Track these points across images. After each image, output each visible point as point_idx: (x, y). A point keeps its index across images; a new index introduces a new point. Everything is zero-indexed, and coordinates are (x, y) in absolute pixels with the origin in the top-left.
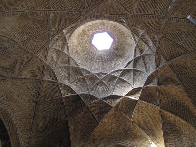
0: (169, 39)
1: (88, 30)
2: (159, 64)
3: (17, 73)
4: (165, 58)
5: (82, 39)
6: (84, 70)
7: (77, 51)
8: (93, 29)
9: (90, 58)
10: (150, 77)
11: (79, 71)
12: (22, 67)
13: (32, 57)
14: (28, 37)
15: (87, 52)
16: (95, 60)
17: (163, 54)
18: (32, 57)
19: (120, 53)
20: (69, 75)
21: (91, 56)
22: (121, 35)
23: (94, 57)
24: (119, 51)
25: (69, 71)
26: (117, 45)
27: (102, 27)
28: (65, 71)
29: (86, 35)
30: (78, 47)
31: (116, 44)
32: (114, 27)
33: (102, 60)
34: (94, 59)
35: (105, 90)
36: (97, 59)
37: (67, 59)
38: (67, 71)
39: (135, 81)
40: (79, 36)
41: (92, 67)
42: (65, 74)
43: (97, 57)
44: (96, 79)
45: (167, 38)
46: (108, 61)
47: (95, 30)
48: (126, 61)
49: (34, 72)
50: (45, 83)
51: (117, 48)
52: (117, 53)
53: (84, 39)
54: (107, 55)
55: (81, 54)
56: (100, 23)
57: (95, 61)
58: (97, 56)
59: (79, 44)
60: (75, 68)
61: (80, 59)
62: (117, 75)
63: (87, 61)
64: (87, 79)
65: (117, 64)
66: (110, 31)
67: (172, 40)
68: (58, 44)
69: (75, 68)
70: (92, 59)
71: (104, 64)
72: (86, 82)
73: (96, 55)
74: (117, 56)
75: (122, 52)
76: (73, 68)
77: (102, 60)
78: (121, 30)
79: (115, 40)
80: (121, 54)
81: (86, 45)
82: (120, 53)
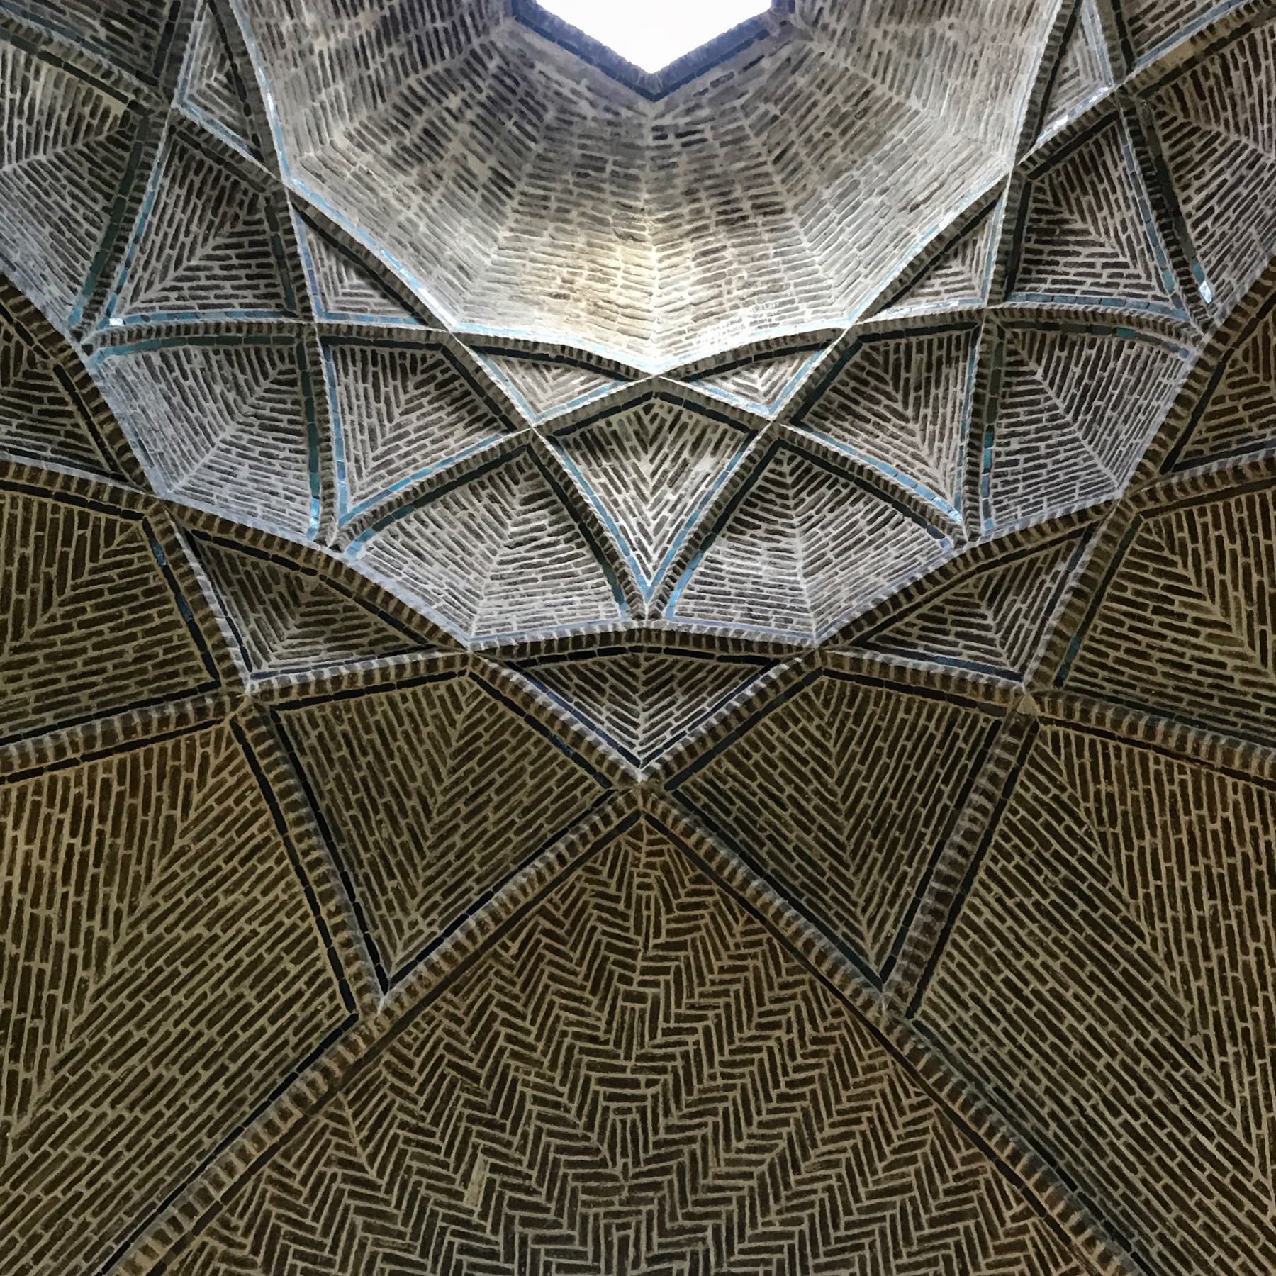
0: (1007, 792)
2: (592, 686)
4: (697, 757)
10: (310, 582)
17: (741, 732)
19: (461, 134)
22: (722, 191)
24: (488, 126)
26: (567, 117)
31: (584, 107)
32: (839, 120)
39: (156, 359)
45: (1021, 776)
48: (379, 217)
51: (531, 107)
52: (454, 102)
67: (1001, 826)
74: (415, 102)
75: (482, 172)
78: (790, 204)
79: (643, 104)
80: (454, 147)
82: (461, 134)
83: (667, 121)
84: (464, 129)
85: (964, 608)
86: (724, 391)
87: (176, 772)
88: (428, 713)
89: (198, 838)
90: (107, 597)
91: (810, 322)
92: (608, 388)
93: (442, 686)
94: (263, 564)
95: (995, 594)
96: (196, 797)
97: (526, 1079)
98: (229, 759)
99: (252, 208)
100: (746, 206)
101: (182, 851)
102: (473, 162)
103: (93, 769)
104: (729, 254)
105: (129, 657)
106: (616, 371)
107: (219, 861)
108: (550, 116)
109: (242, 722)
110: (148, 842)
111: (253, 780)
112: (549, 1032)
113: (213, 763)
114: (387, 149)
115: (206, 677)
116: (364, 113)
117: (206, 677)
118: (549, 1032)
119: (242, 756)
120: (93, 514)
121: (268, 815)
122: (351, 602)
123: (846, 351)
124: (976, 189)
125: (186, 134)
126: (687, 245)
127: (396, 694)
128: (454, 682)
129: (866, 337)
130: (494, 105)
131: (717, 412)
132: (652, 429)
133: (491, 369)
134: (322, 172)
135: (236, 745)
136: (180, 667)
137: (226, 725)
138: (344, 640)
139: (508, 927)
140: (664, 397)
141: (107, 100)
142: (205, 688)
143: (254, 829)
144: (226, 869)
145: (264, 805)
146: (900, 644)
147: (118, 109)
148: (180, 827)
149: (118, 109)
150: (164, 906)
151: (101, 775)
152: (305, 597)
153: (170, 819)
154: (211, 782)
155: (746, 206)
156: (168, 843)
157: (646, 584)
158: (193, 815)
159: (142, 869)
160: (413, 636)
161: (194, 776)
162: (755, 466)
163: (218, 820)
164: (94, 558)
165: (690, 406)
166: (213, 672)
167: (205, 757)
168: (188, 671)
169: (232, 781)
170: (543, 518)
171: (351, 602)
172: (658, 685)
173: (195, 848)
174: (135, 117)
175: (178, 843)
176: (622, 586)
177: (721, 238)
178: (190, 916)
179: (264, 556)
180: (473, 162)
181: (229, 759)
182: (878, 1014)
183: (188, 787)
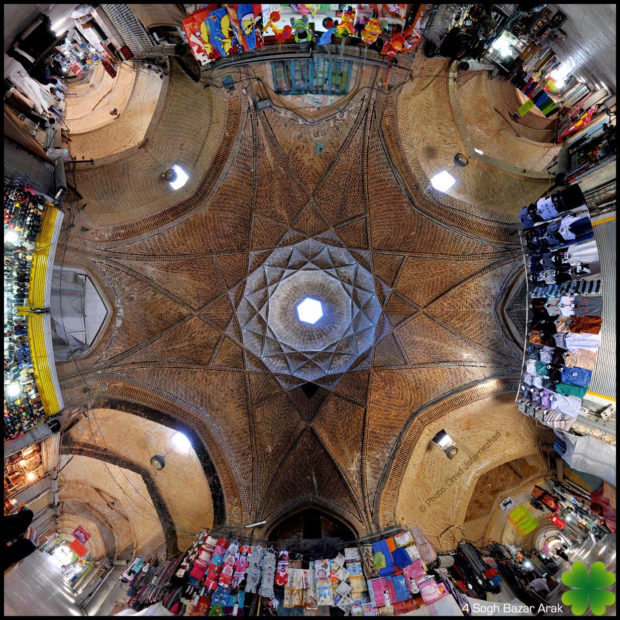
3: (206, 360)
4: (363, 249)
5: (286, 320)
6: (307, 353)
12: (211, 351)
14: (205, 302)
15: (301, 333)
16: (316, 337)
19: (337, 311)
20: (288, 365)
22: (323, 289)
23: (312, 334)
24: (334, 310)
25: (286, 359)
30: (286, 331)
36: (317, 335)
40: (281, 318)
43: (316, 333)
44: (329, 356)
46: (331, 330)
47: (294, 301)
50: (252, 377)
53: (289, 319)
55: (294, 337)
61: (295, 344)
62: (351, 332)
64: (317, 361)
65: (343, 325)
72: (316, 365)
73: (313, 331)
74: (337, 317)
76: (290, 355)
82: (337, 311)
85: (331, 241)
86: (335, 275)
91: (325, 274)
92: (345, 284)
95: (328, 239)
97: (402, 237)
106: (343, 284)
112: (397, 239)
118: (397, 239)
124: (303, 272)
125: (354, 331)
129: (321, 268)
133: (351, 294)
134: (348, 319)
138: (381, 286)
139: (391, 250)
146: (339, 242)
157: (353, 267)
172: (362, 257)
176: (357, 268)
182: (368, 215)
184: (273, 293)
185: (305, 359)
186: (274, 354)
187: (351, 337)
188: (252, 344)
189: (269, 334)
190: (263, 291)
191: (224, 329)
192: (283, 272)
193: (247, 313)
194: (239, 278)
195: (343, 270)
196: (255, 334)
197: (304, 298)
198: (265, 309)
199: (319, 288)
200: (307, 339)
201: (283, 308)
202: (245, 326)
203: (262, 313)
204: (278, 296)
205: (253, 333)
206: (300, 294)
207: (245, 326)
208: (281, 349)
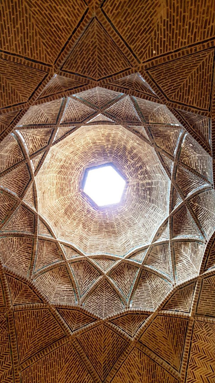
1: (96, 222)
7: (144, 226)
8: (88, 216)
9: (148, 192)
11: (178, 213)
13: (138, 349)
18: (138, 349)
21: (145, 191)
27: (77, 206)
28: (182, 251)
29: (108, 221)
30: (136, 227)
32: (62, 189)
33: (141, 167)
34: (148, 184)
35: (191, 145)
36: (145, 178)
37: (158, 247)
38: (183, 246)
41: (161, 184)
42: (189, 251)
43: (141, 180)
46: (136, 155)
47: (88, 211)
49: (176, 337)
53: (117, 219)
54: (127, 161)
55: (147, 215)
56: (71, 213)
57: (150, 181)
58: (138, 180)
59: (130, 226)
60: (174, 225)
63: (157, 198)
64: (188, 191)
66: (75, 188)
68: (128, 280)
69: (174, 225)
70: (150, 189)
71: (145, 159)
77: (141, 167)
78: (58, 176)
79: (87, 167)
80: (104, 141)
81: (127, 210)
83: (82, 168)
84: (105, 144)
87: (52, 49)
88: (26, 91)
89: (36, 40)
90: (91, 65)
93: (29, 97)
94: (73, 87)
96: (44, 47)
98: (46, 59)
99: (122, 119)
100: (63, 170)
101: (36, 35)
102: (100, 141)
103: (65, 40)
104: (58, 163)
105: (78, 60)
107: (29, 40)
108: (96, 155)
109: (51, 68)
110: (43, 32)
111: (38, 60)
113: (48, 56)
114: (112, 135)
115: (63, 69)
116: (119, 137)
117: (63, 69)
119: (45, 62)
120: (105, 76)
121: (30, 57)
122: (55, 93)
123: (31, 176)
126: (65, 159)
127: (34, 90)
128: (28, 99)
129: (31, 179)
130: (104, 151)
131: (38, 152)
132: (43, 141)
135: (47, 63)
136: (69, 66)
137: (52, 64)
138: (50, 89)
140: (46, 146)
141: (152, 122)
142: (62, 68)
143: (30, 52)
144: (26, 40)
145: (33, 58)
147: (150, 121)
148: (41, 39)
149: (150, 121)
150: (29, 23)
151: (63, 40)
152: (62, 87)
153: (44, 39)
154: (45, 52)
155: (63, 170)
156: (40, 34)
158: (42, 43)
159: (39, 26)
160: (41, 98)
161: (48, 51)
162: (25, 154)
163: (37, 47)
164: (98, 69)
165: (42, 149)
166: (63, 71)
167: (50, 56)
168: (67, 67)
169: (42, 56)
170: (43, 120)
171: (55, 93)
173: (35, 38)
174: (147, 122)
175: (38, 36)
177: (62, 164)
178: (23, 26)
179: (75, 88)
180: (100, 141)
181: (46, 59)
183: (47, 47)
184: (75, 251)
185: (182, 211)
186: (169, 258)
187: (149, 130)
188: (153, 292)
189: (140, 258)
190: (72, 268)
191: (127, 342)
192: (42, 240)
193: (106, 295)
194: (52, 317)
195: (28, 148)
196: (138, 285)
197: (83, 193)
198: (101, 262)
199: (66, 174)
200: (150, 195)
201: (100, 231)
202: (124, 303)
203: (106, 268)
204: (81, 239)
205: (135, 288)
206: (78, 203)
207: (124, 303)
208: (165, 244)
